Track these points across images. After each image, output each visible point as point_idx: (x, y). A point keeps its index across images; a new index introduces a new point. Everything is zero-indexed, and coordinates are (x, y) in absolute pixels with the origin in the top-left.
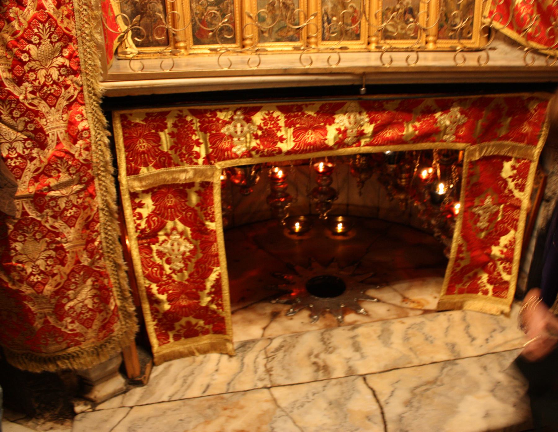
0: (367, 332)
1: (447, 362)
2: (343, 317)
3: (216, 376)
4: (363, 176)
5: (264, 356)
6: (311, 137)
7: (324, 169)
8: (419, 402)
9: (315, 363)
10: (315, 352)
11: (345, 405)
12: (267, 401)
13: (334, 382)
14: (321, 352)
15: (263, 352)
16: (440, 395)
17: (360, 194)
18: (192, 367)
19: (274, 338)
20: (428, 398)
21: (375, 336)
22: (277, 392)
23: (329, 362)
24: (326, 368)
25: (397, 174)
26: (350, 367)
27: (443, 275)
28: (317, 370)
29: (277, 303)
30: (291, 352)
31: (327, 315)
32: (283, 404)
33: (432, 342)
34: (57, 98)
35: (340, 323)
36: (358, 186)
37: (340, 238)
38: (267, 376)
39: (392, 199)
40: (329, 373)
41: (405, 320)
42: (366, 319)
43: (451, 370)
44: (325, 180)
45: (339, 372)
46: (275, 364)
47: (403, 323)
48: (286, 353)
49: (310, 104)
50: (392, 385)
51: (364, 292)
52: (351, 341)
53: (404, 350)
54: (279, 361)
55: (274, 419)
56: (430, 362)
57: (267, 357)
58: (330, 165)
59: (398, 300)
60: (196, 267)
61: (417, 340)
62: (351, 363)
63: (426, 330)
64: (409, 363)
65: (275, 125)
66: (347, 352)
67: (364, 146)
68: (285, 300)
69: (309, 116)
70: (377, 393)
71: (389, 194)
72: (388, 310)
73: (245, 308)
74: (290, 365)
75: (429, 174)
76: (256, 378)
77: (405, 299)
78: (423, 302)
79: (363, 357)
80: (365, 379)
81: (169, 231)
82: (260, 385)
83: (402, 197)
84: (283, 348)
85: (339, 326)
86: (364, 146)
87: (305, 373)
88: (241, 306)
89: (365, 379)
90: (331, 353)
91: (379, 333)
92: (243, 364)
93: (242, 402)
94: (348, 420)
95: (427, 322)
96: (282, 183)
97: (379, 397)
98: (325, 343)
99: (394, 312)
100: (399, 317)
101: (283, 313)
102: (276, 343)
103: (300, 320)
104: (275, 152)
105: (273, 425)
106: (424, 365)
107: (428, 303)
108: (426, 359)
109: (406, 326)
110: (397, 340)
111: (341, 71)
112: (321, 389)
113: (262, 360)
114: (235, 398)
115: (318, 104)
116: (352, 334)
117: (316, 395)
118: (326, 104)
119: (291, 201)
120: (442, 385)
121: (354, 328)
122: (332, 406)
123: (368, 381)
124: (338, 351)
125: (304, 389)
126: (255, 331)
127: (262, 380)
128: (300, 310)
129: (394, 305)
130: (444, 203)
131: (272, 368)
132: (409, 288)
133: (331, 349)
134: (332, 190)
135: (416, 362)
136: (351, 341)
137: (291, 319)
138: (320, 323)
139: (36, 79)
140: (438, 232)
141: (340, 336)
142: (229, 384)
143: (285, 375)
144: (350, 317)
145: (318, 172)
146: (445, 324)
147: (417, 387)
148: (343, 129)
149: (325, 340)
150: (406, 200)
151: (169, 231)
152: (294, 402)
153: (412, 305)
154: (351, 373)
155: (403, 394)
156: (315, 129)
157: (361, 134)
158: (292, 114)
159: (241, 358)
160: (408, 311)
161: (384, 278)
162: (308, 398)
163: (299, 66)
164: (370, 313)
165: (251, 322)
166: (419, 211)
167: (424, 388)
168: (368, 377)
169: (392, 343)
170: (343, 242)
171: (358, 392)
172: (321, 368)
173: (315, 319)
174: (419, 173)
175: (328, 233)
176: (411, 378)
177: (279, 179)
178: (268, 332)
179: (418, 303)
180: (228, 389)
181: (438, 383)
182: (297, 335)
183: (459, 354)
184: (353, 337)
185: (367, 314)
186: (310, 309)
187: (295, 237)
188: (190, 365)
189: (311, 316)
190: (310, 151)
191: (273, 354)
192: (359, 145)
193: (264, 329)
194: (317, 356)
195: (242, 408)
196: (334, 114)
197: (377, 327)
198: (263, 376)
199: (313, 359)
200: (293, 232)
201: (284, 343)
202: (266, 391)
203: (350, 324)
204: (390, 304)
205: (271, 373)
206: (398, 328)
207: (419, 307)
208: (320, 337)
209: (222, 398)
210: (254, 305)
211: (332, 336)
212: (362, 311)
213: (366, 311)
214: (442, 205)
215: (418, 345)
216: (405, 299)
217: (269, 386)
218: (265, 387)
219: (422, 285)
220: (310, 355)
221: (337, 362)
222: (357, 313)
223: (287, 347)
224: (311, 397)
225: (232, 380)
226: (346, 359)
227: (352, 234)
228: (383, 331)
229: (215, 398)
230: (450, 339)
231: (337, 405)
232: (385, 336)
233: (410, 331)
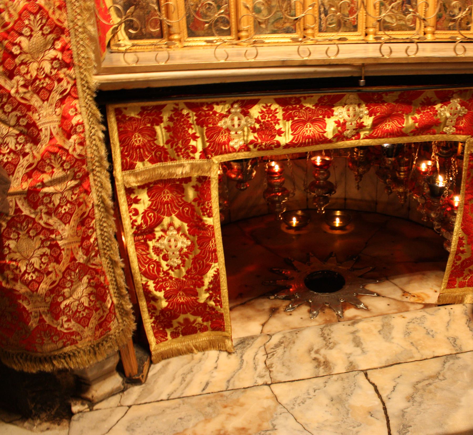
0: (368, 327)
1: (449, 356)
2: (343, 312)
3: (215, 374)
4: (361, 170)
5: (264, 353)
6: (310, 130)
7: (321, 162)
8: (422, 397)
9: (315, 359)
10: (316, 348)
11: (348, 400)
12: (267, 398)
13: (335, 377)
14: (322, 348)
15: (263, 348)
16: (443, 389)
17: (358, 188)
18: (191, 364)
19: (273, 335)
20: (430, 392)
21: (375, 331)
22: (277, 389)
23: (329, 358)
24: (326, 364)
25: (396, 167)
26: (351, 363)
27: (444, 270)
28: (318, 367)
29: (275, 298)
30: (291, 348)
31: (327, 310)
32: (284, 401)
33: (433, 336)
35: (340, 319)
36: (356, 180)
37: (338, 232)
38: (268, 373)
39: (391, 192)
40: (330, 369)
41: (405, 314)
42: (366, 314)
43: (453, 364)
44: (323, 174)
46: (274, 360)
47: (403, 317)
48: (286, 349)
49: (308, 97)
50: (394, 380)
51: (364, 286)
52: (351, 337)
53: (406, 345)
54: (279, 357)
55: (275, 416)
56: (432, 356)
57: (267, 354)
58: (327, 159)
59: (398, 295)
60: (194, 263)
61: (418, 335)
62: (352, 359)
63: (427, 324)
64: (411, 358)
65: (273, 118)
66: (347, 347)
67: (364, 138)
68: (284, 296)
69: (308, 108)
70: (379, 388)
71: (388, 188)
73: (243, 304)
74: (290, 361)
75: (428, 166)
76: (256, 375)
77: (405, 293)
78: (423, 296)
79: (363, 352)
80: (366, 375)
81: (166, 227)
82: (260, 382)
83: (401, 190)
84: (283, 345)
85: (339, 321)
86: (364, 138)
87: (306, 369)
88: (239, 303)
89: (366, 375)
90: (331, 349)
91: (380, 327)
92: (242, 361)
93: (242, 400)
94: (350, 416)
95: (428, 316)
96: (279, 177)
97: (381, 392)
98: (325, 339)
99: (394, 306)
100: (400, 311)
101: (282, 309)
102: (275, 340)
103: (299, 316)
104: (273, 146)
105: (274, 423)
106: (427, 359)
107: (428, 297)
108: (428, 353)
109: (407, 320)
110: (397, 334)
111: (340, 63)
112: (322, 385)
113: (261, 357)
114: (235, 395)
115: (316, 96)
116: (352, 329)
117: (317, 391)
118: (325, 96)
119: (288, 196)
120: (445, 379)
121: (353, 323)
122: (333, 402)
123: (369, 376)
124: (338, 346)
125: (304, 385)
126: (254, 327)
127: (262, 377)
128: (299, 306)
129: (394, 299)
130: (444, 196)
131: (272, 364)
132: (409, 282)
133: (332, 345)
134: (330, 183)
135: (418, 357)
136: (351, 337)
137: (291, 315)
138: (320, 319)
140: (438, 226)
141: (340, 331)
142: (229, 381)
143: (285, 370)
144: (350, 312)
145: (316, 166)
146: (447, 318)
147: (418, 382)
148: (342, 121)
149: (326, 335)
150: (405, 193)
151: (166, 227)
152: (295, 399)
153: (412, 300)
154: (352, 368)
155: (405, 389)
156: (313, 122)
157: (361, 127)
158: (290, 107)
159: (240, 355)
160: (409, 305)
161: (384, 272)
162: (309, 394)
163: (296, 58)
164: (369, 308)
165: (249, 318)
166: (419, 204)
167: (427, 382)
168: (369, 372)
169: (393, 338)
170: (341, 236)
171: (360, 387)
172: (322, 364)
173: (314, 315)
174: (418, 165)
175: (326, 228)
176: (412, 373)
177: (276, 173)
178: (267, 329)
179: (418, 297)
180: (228, 387)
181: (441, 377)
182: (297, 331)
183: (460, 348)
184: (353, 333)
185: (367, 309)
186: (309, 304)
187: (292, 232)
188: (189, 363)
189: (310, 312)
190: (308, 144)
191: (272, 350)
192: (359, 138)
193: (263, 325)
194: (317, 352)
195: (242, 405)
196: (333, 106)
197: (378, 322)
198: (263, 373)
199: (313, 355)
200: (290, 227)
201: (284, 339)
202: (266, 387)
203: (350, 319)
204: (390, 298)
205: (271, 369)
206: (399, 322)
207: (420, 302)
208: (320, 333)
209: (222, 396)
211: (332, 332)
212: (362, 306)
214: (442, 198)
215: (419, 340)
216: (405, 293)
217: (269, 382)
218: (266, 384)
219: (422, 279)
220: (310, 351)
221: (338, 358)
222: (356, 308)
223: (286, 343)
225: (232, 377)
226: (346, 354)
227: (350, 228)
228: (383, 326)
229: (215, 396)
230: (451, 333)
231: (338, 401)
232: (385, 331)
233: (411, 325)
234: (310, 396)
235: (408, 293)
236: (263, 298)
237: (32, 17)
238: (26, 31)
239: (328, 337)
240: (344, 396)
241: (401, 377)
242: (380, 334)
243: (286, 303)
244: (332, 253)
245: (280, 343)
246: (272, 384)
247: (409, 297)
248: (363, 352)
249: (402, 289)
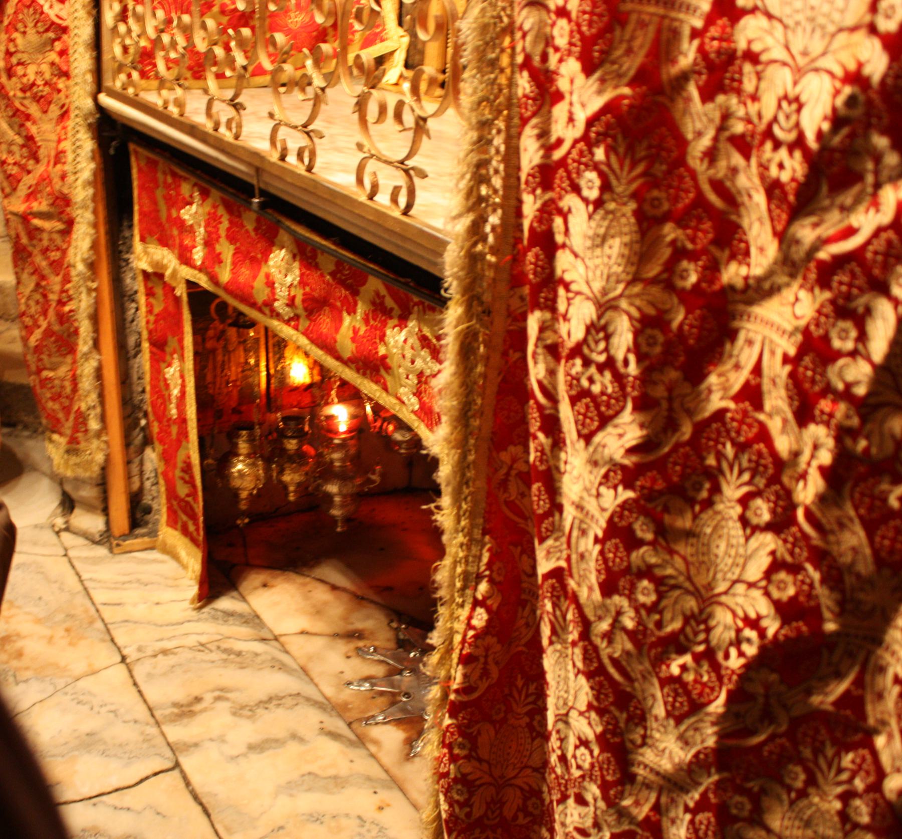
10: (229, 695)
14: (233, 702)
15: (219, 637)
34: (50, 103)
45: (175, 733)
57: (202, 645)
90: (234, 714)
91: (332, 772)
101: (361, 644)
110: (307, 802)
112: (127, 718)
113: (192, 641)
117: (112, 715)
131: (175, 654)
133: (250, 713)
137: (348, 657)
139: (25, 75)
149: (275, 702)
168: (176, 773)
169: (291, 795)
184: (294, 736)
193: (302, 633)
194: (218, 699)
199: (208, 698)
202: (119, 659)
210: (372, 606)
224: (104, 710)
225: (136, 622)
228: (335, 778)
234: (96, 709)
236: (387, 616)
237: (26, 11)
238: (20, 26)
239: (271, 706)
240: (102, 748)
241: (159, 817)
242: (303, 775)
245: (239, 654)
246: (127, 664)
248: (234, 758)
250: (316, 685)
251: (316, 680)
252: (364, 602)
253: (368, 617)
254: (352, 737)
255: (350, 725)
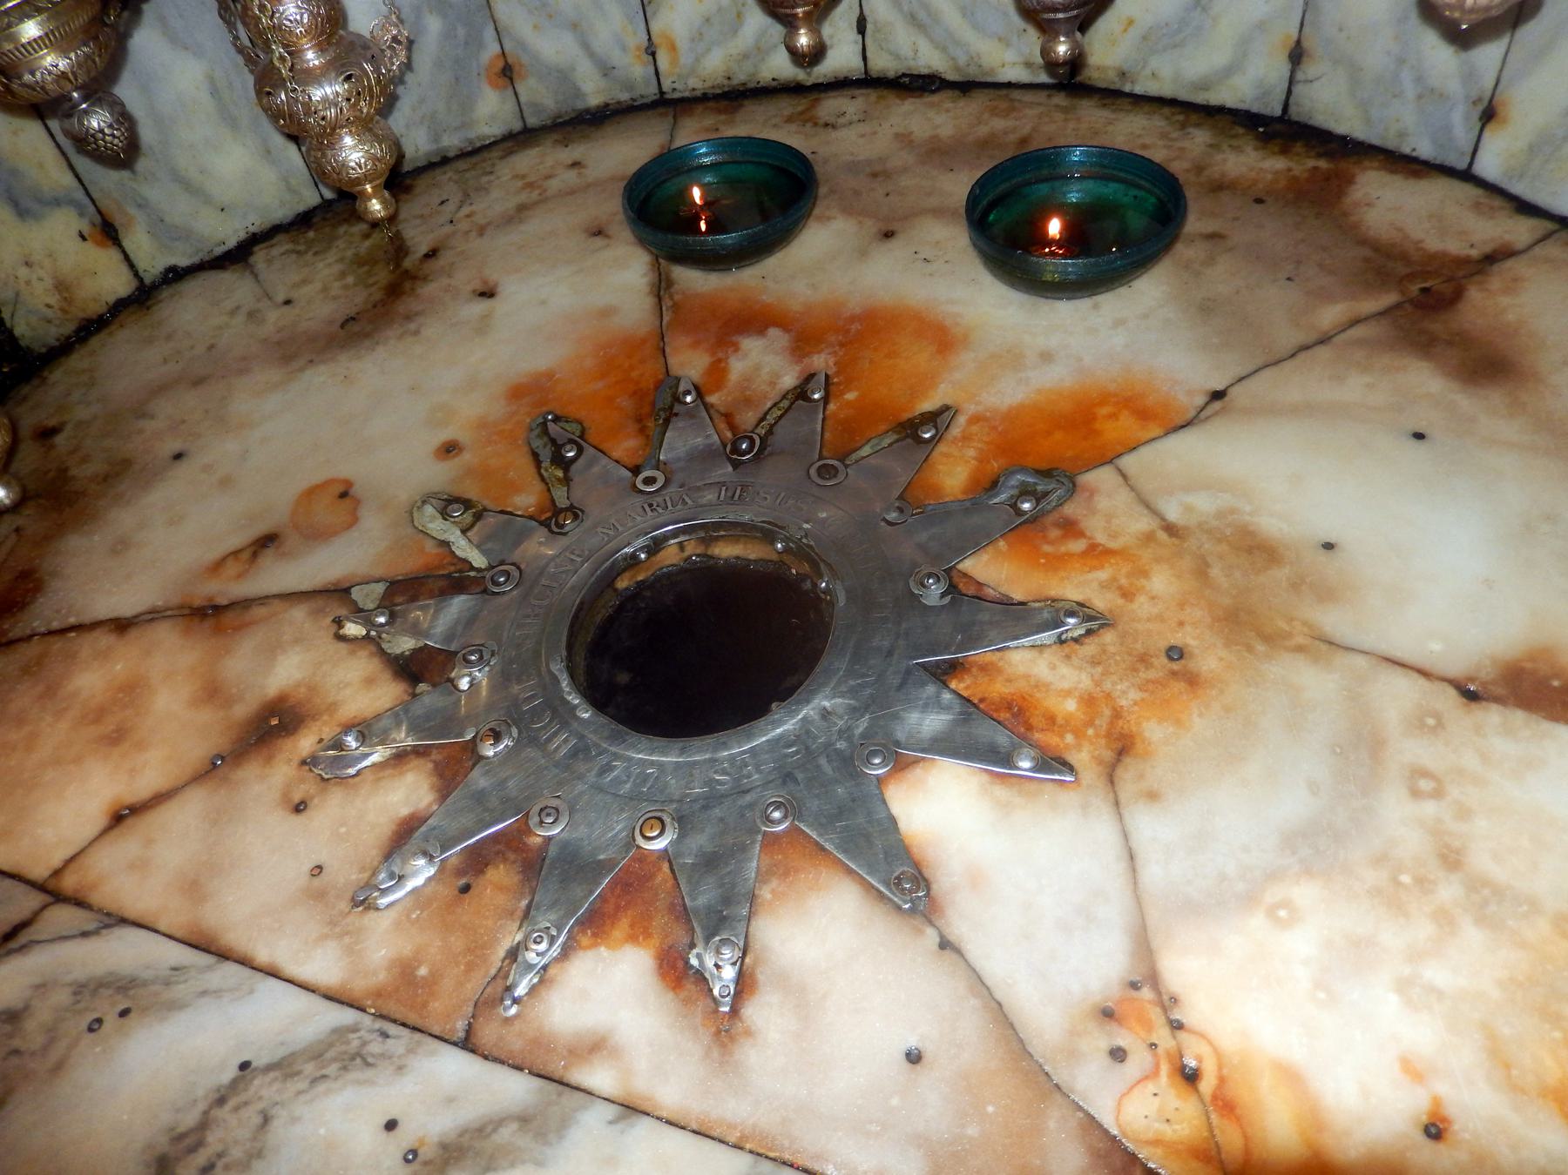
2: (565, 953)
72: (914, 1057)
77: (1140, 1001)
101: (306, 743)
129: (1001, 1017)
137: (299, 808)
164: (753, 1011)
204: (978, 983)
208: (190, 1119)
213: (745, 984)
235: (1168, 1002)
243: (387, 693)
244: (932, 418)
247: (1139, 1060)
249: (1144, 948)
250: (273, 973)
251: (262, 956)
252: (229, 618)
253: (272, 650)
254: (514, 1088)
255: (467, 1044)
